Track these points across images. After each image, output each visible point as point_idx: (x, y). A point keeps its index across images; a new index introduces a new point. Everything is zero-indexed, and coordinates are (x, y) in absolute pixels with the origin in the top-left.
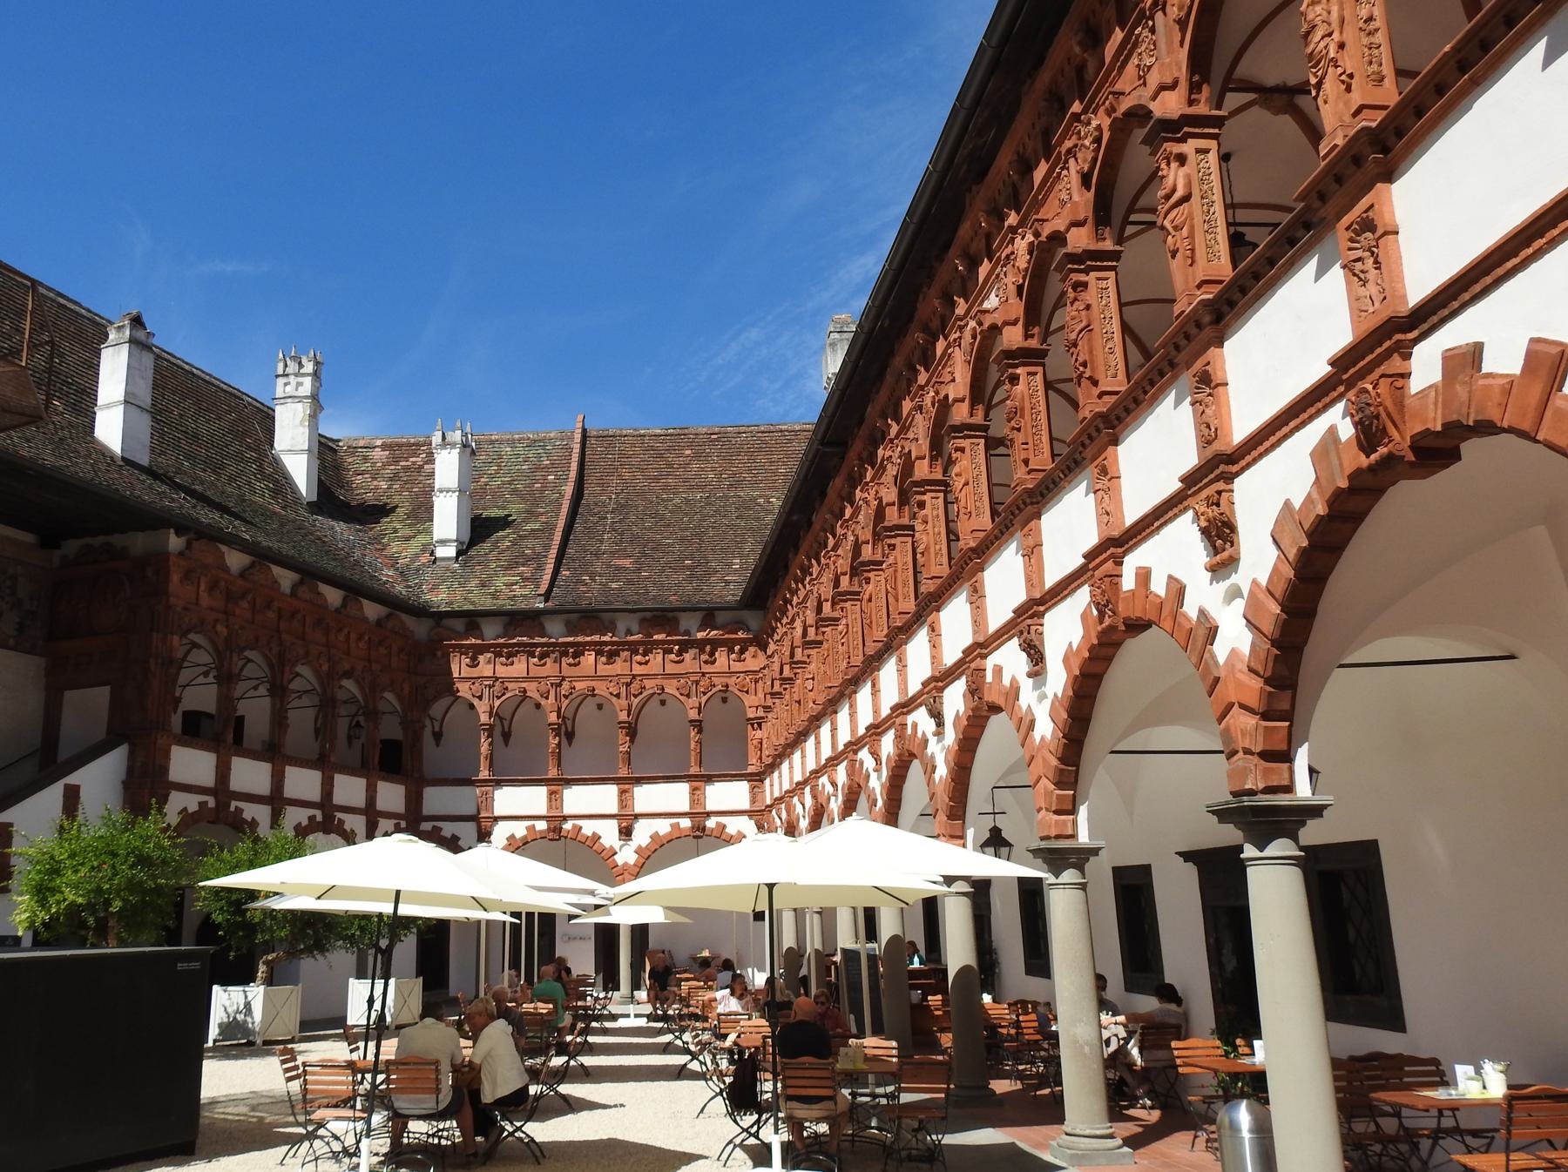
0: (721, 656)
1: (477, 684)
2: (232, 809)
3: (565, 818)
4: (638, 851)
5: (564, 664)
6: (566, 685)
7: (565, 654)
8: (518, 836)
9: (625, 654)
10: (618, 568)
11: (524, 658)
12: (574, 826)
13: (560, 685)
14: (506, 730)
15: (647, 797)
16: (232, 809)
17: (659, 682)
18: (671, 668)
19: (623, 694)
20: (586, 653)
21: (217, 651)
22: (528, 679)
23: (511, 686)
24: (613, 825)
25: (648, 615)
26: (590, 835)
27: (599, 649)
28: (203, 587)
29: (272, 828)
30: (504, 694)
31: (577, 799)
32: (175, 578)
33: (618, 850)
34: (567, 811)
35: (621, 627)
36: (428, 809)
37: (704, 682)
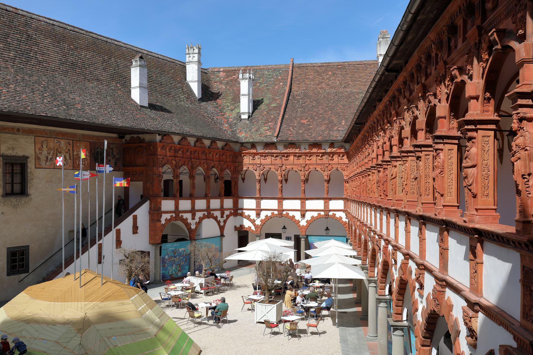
0: (336, 157)
1: (255, 166)
2: (180, 216)
3: (284, 210)
4: (307, 221)
5: (283, 160)
6: (284, 167)
7: (284, 156)
8: (269, 215)
9: (303, 157)
10: (302, 124)
11: (270, 157)
12: (286, 213)
13: (282, 167)
14: (265, 178)
15: (310, 204)
16: (180, 216)
17: (315, 166)
18: (319, 162)
19: (303, 170)
20: (291, 156)
21: (173, 169)
22: (271, 164)
23: (266, 167)
25: (312, 143)
26: (292, 216)
27: (295, 154)
28: (167, 150)
29: (192, 219)
30: (264, 169)
31: (287, 204)
32: (159, 149)
33: (300, 221)
34: (284, 208)
35: (302, 147)
37: (330, 167)
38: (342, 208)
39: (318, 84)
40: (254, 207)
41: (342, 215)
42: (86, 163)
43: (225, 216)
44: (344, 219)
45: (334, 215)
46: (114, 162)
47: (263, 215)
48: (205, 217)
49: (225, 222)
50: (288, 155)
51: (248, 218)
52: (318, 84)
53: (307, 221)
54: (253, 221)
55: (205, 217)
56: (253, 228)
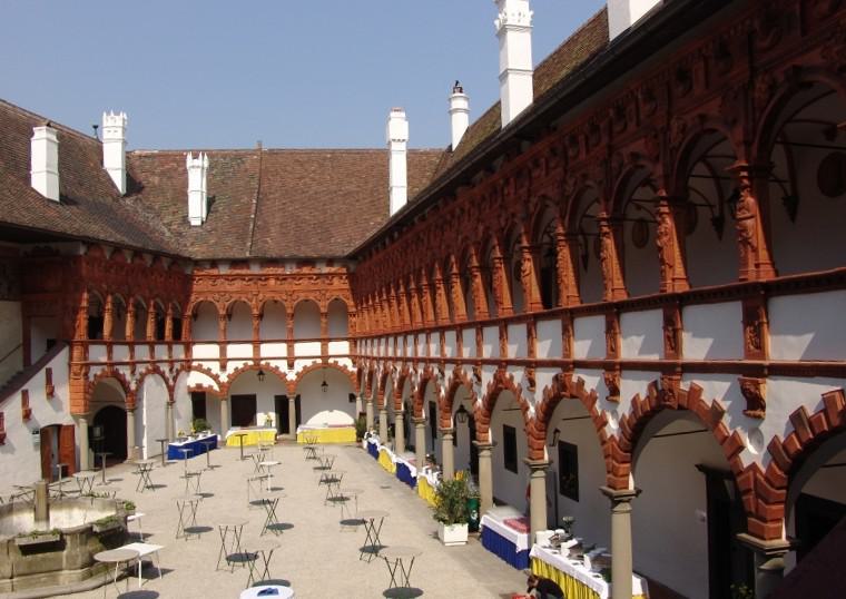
0: (336, 281)
3: (262, 359)
4: (297, 374)
9: (290, 280)
15: (300, 349)
18: (313, 288)
24: (285, 362)
27: (277, 277)
31: (267, 350)
38: (347, 352)
39: (300, 179)
40: (218, 356)
41: (348, 362)
43: (174, 370)
44: (351, 368)
45: (336, 363)
47: (231, 367)
48: (149, 372)
49: (175, 379)
50: (267, 277)
51: (208, 372)
52: (300, 179)
53: (297, 374)
54: (216, 378)
56: (216, 388)
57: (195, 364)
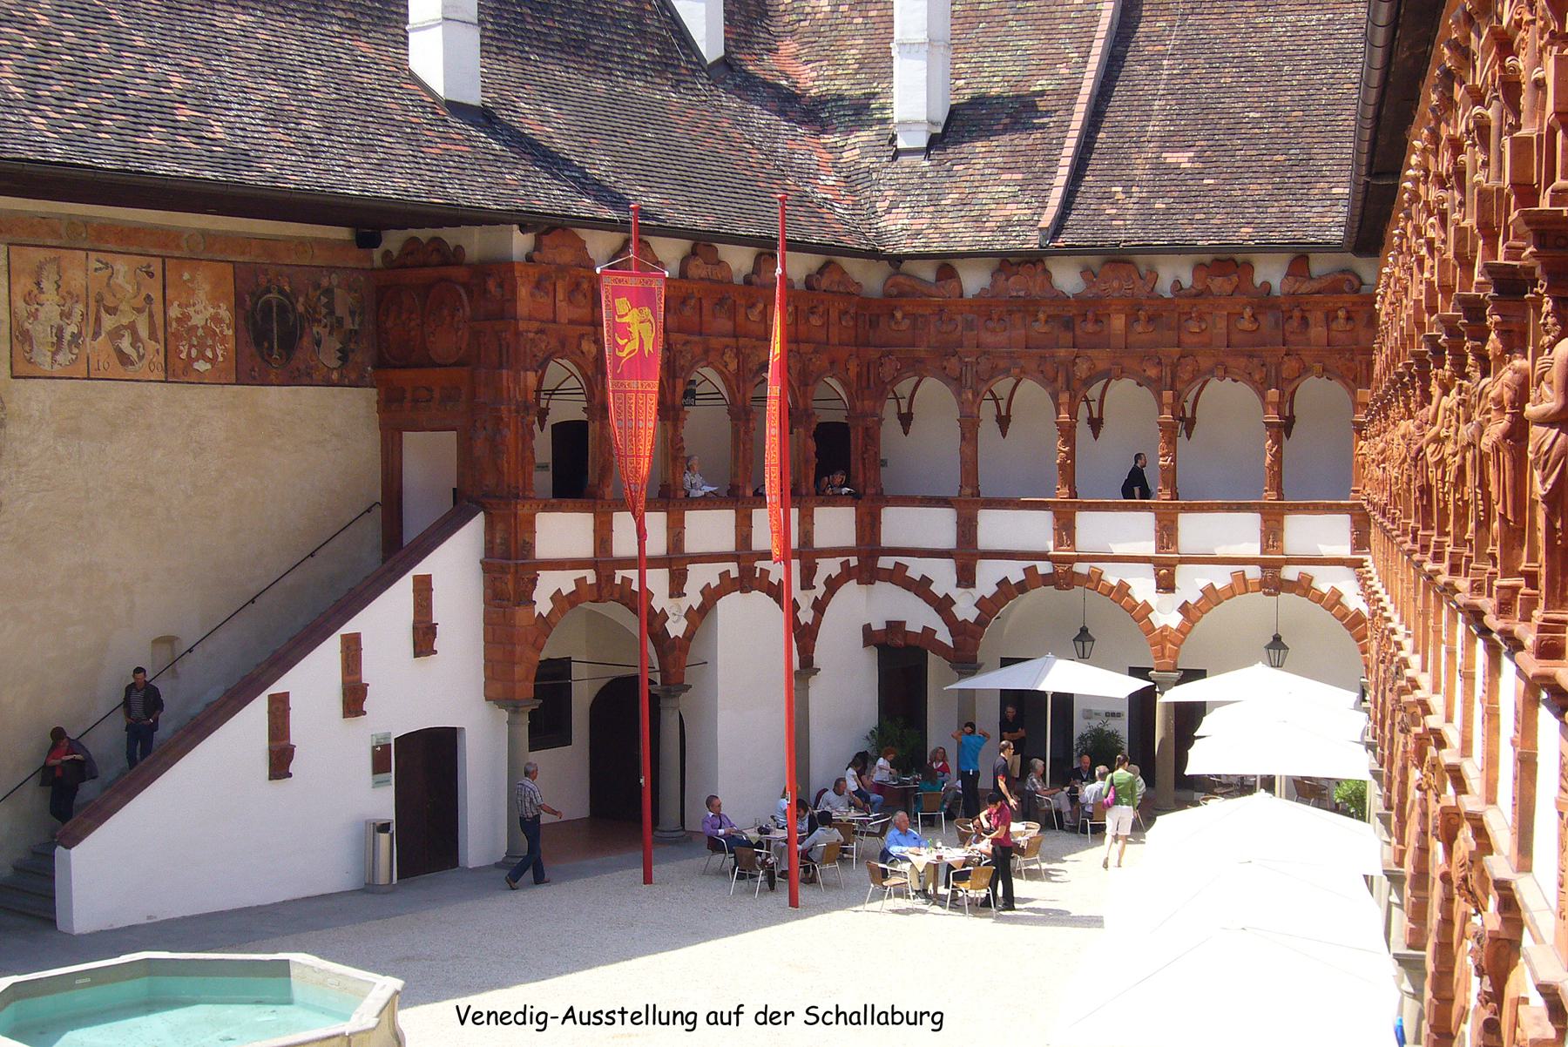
2: (618, 581)
21: (584, 375)
25: (1207, 258)
28: (560, 296)
29: (671, 596)
32: (523, 292)
36: (888, 538)
42: (219, 353)
43: (819, 581)
46: (339, 346)
47: (989, 575)
48: (728, 585)
49: (819, 607)
51: (921, 587)
54: (943, 606)
55: (728, 585)
56: (944, 636)
57: (886, 562)
